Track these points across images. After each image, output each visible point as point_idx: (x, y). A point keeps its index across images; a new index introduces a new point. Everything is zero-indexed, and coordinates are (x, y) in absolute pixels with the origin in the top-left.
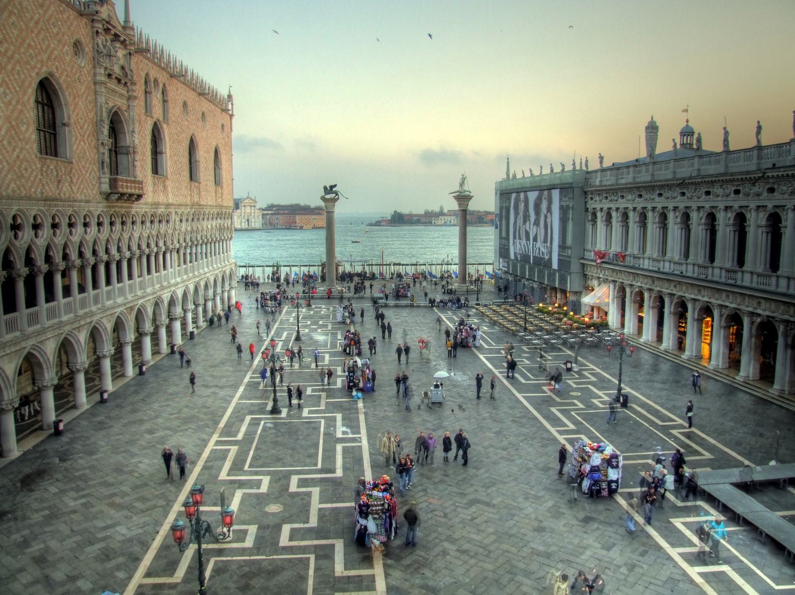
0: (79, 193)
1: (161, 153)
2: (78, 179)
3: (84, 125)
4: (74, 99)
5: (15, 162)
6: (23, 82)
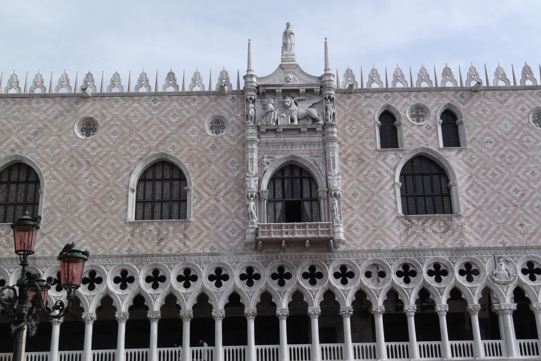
0: (200, 247)
1: (451, 187)
2: (199, 235)
3: (217, 185)
4: (200, 166)
5: (93, 230)
6: (119, 168)
